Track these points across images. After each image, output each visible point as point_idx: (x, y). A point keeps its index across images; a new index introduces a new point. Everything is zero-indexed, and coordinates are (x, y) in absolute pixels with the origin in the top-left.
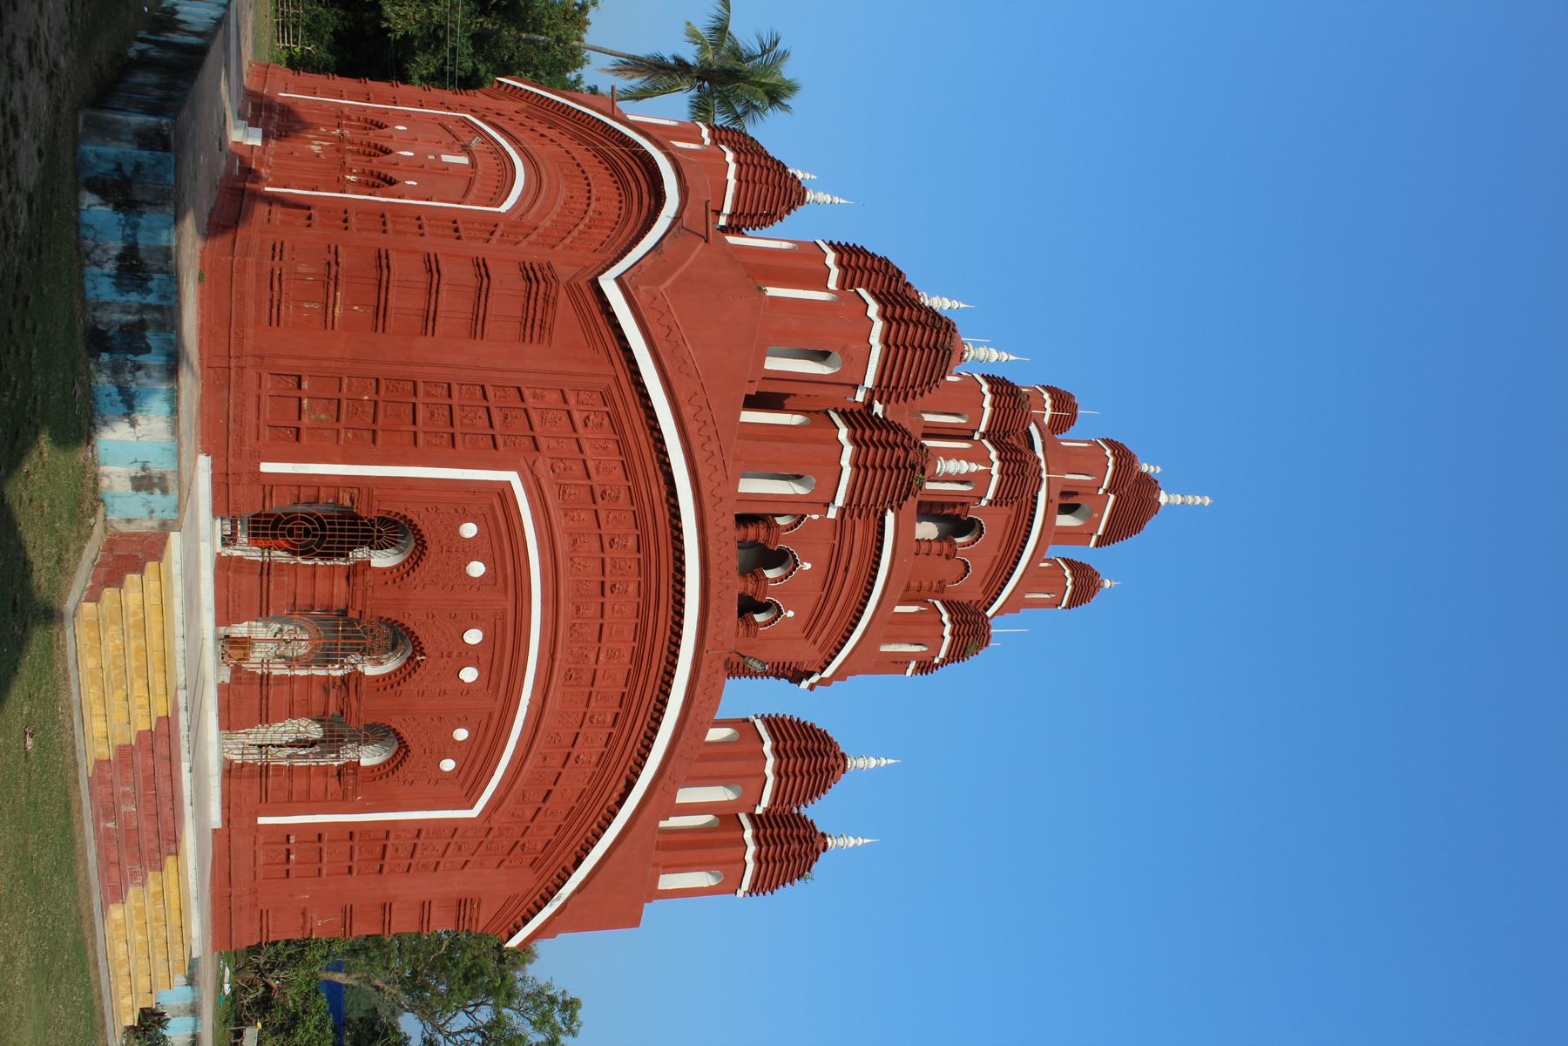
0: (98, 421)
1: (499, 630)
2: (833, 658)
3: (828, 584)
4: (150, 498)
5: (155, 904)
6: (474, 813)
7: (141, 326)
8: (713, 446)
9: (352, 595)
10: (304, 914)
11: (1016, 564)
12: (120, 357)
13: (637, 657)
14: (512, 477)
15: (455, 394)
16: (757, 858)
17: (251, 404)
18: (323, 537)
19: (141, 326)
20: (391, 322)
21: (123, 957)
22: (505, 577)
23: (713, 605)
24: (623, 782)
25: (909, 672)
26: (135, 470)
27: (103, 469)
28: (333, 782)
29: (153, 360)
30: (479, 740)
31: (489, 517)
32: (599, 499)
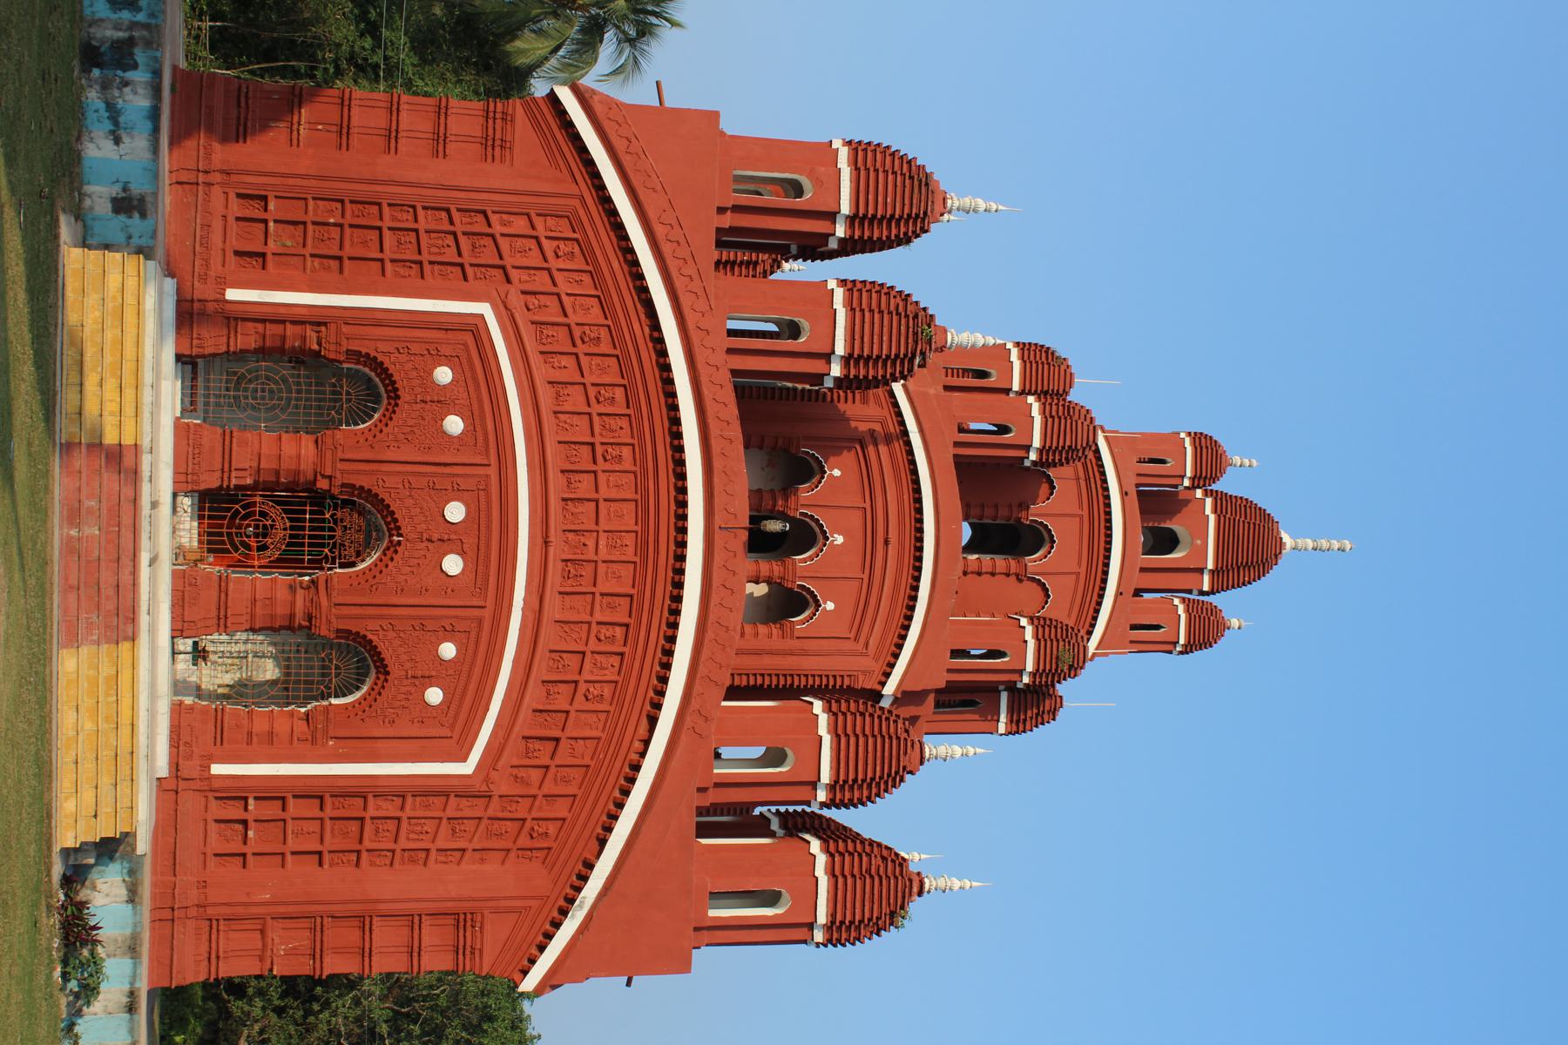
0: (85, 138)
1: (483, 507)
2: (892, 666)
3: (868, 563)
4: (129, 222)
5: (107, 695)
6: (467, 768)
7: (131, 42)
8: (690, 270)
9: (320, 454)
10: (262, 932)
11: (1104, 581)
12: (109, 73)
13: (642, 547)
14: (484, 309)
15: (421, 218)
16: (831, 872)
17: (217, 225)
18: (289, 399)
19: (131, 42)
20: (354, 140)
21: (72, 733)
22: (486, 434)
23: (717, 464)
24: (644, 723)
25: (1002, 728)
26: (116, 190)
27: (88, 189)
28: (301, 727)
29: (140, 76)
30: (469, 659)
31: (464, 361)
32: (579, 342)
